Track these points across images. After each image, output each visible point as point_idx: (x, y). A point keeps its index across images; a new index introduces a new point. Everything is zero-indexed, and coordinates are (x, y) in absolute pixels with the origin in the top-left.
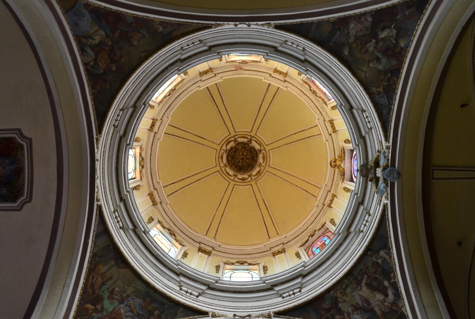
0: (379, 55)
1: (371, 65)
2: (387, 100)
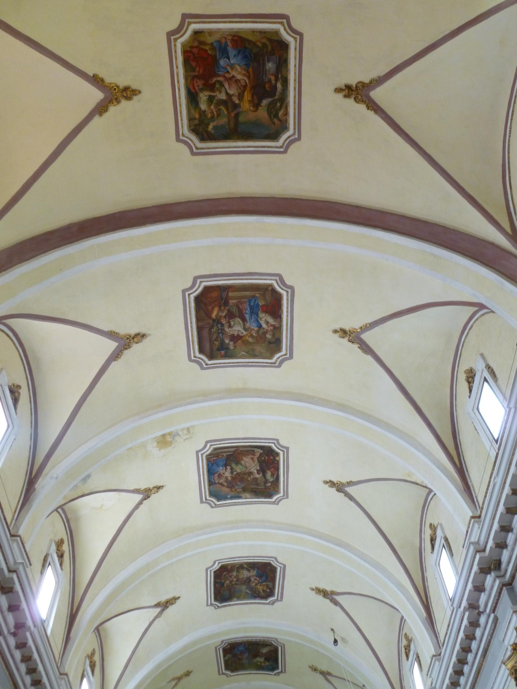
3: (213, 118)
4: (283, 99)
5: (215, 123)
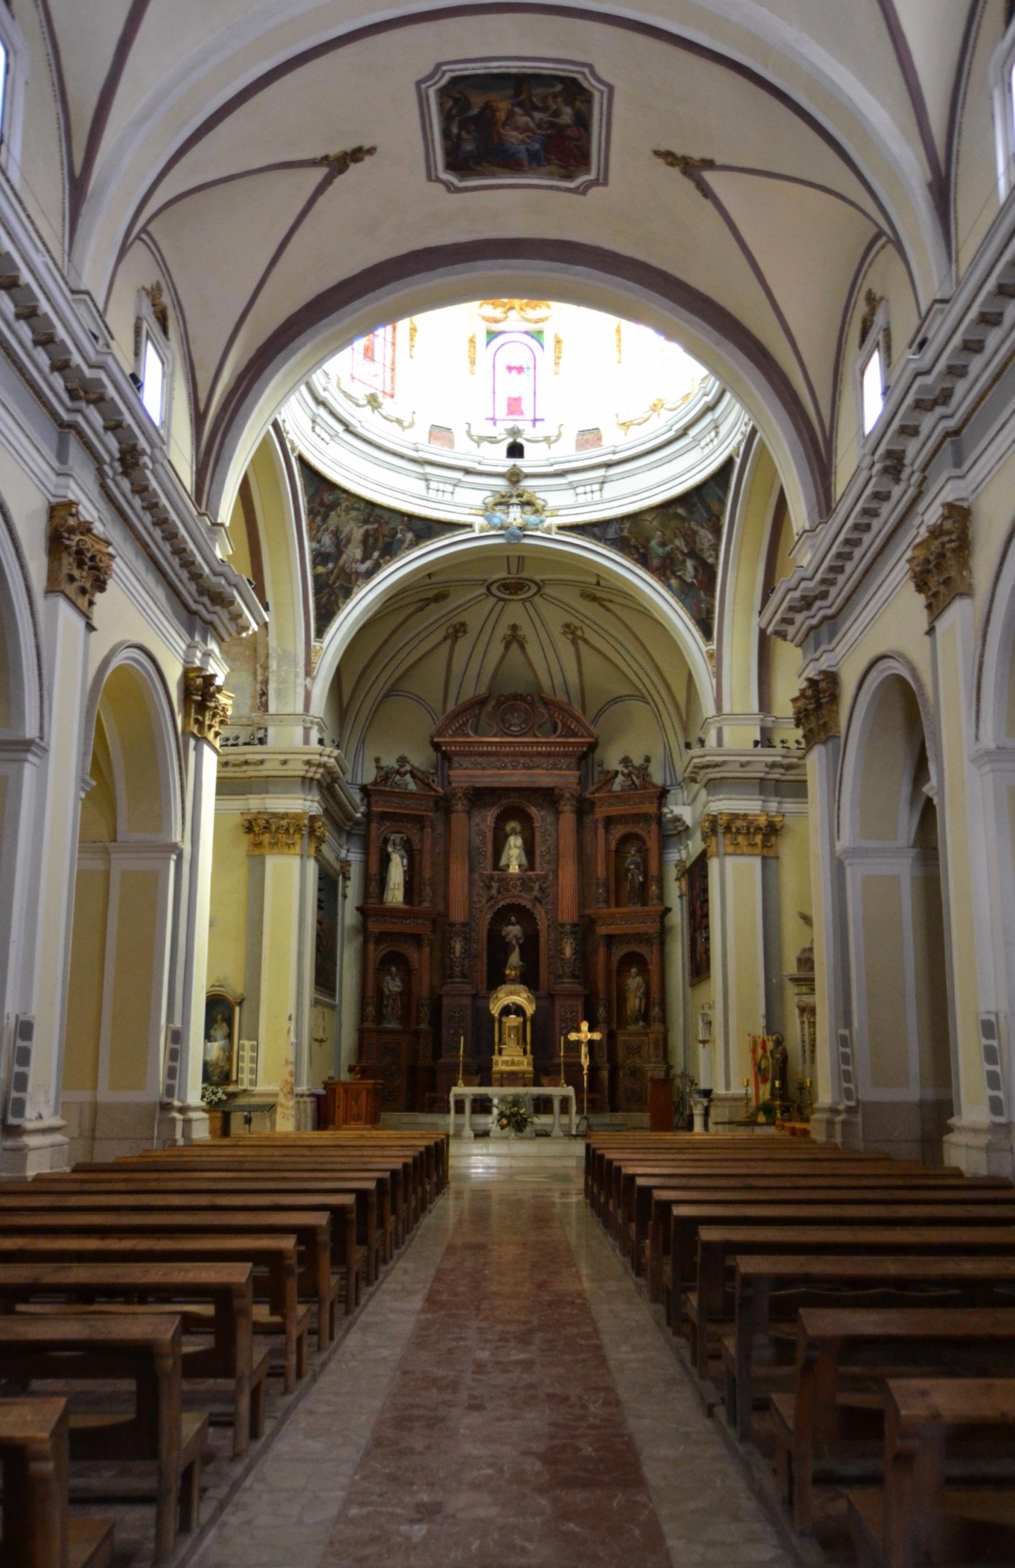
0: (668, 548)
1: (659, 533)
2: (611, 537)
3: (555, 96)
4: (447, 118)
5: (551, 90)
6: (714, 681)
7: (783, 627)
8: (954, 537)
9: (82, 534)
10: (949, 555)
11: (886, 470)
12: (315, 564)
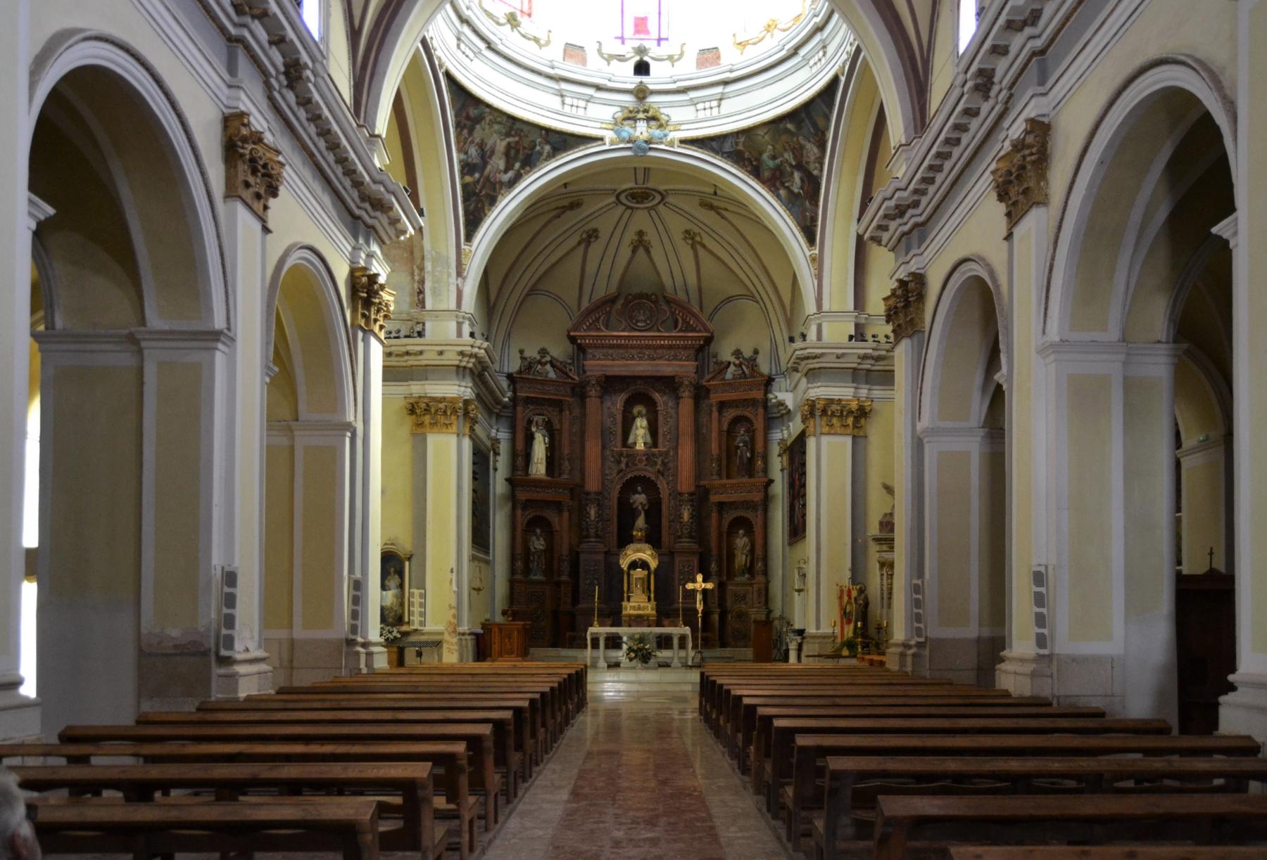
0: (778, 161)
1: (770, 147)
6: (816, 282)
7: (879, 233)
8: (1034, 150)
9: (254, 143)
10: (1029, 167)
11: (977, 88)
12: (463, 174)
